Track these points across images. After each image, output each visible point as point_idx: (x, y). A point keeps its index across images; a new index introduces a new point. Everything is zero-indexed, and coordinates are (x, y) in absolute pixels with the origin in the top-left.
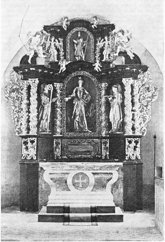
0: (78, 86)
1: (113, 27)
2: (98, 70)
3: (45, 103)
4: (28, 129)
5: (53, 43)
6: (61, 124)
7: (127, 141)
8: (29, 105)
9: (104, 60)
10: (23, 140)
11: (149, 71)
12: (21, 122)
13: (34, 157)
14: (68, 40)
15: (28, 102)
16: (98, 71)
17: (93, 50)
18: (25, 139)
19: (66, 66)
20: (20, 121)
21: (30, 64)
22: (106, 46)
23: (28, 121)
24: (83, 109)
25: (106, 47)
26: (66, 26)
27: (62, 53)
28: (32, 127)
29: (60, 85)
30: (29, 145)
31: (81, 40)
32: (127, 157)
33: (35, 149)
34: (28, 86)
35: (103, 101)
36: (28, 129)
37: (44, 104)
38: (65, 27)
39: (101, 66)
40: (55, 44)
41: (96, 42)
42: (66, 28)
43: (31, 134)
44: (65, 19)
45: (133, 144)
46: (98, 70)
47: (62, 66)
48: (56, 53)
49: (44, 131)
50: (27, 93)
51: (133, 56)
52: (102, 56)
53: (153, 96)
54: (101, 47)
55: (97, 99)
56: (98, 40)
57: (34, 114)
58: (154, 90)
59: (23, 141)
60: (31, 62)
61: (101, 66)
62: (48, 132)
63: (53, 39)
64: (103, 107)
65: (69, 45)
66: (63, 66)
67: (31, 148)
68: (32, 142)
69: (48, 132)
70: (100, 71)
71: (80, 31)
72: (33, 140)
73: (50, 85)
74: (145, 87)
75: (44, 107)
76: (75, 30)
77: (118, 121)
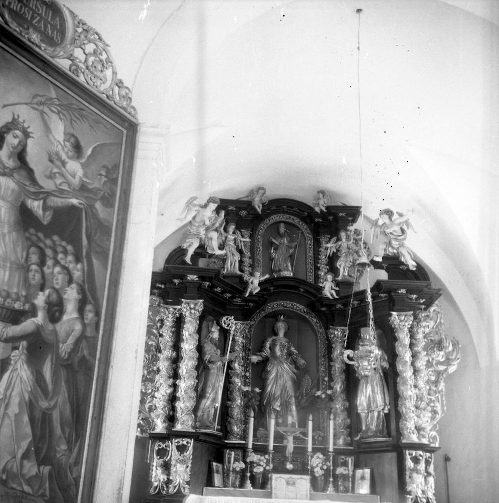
0: (276, 334)
1: (353, 213)
2: (332, 295)
3: (212, 360)
4: (171, 419)
5: (231, 237)
6: (242, 415)
7: (408, 457)
8: (176, 361)
9: (340, 278)
10: (156, 445)
11: (436, 305)
12: (150, 404)
13: (184, 488)
14: (259, 237)
15: (174, 354)
16: (331, 297)
17: (311, 260)
18: (160, 443)
19: (260, 284)
20: (148, 401)
21: (189, 265)
22: (344, 250)
23: (173, 399)
24: (289, 384)
25: (343, 252)
26: (261, 205)
27: (247, 261)
28: (182, 412)
29: (243, 326)
30: (174, 454)
31: (285, 240)
32: (411, 497)
33: (187, 467)
34: (177, 318)
35: (338, 368)
36: (171, 419)
37: (210, 362)
38: (259, 207)
39: (337, 289)
40: (235, 240)
41: (317, 244)
42: (261, 208)
43: (179, 427)
44: (260, 191)
45: (422, 466)
46: (332, 295)
47: (252, 283)
48: (237, 257)
49: (207, 427)
50: (173, 332)
51: (415, 264)
52: (334, 270)
53: (448, 362)
54: (331, 254)
55: (322, 365)
56: (323, 239)
57: (185, 385)
58: (451, 348)
59: (156, 448)
60: (191, 261)
61: (337, 289)
62: (214, 429)
63: (232, 228)
64: (339, 380)
65: (261, 248)
66: (254, 284)
67: (178, 465)
68: (181, 449)
69: (214, 429)
70: (336, 297)
71: (284, 222)
72: (185, 443)
73: (230, 318)
74: (431, 340)
75: (208, 369)
76: (275, 218)
77: (379, 412)
